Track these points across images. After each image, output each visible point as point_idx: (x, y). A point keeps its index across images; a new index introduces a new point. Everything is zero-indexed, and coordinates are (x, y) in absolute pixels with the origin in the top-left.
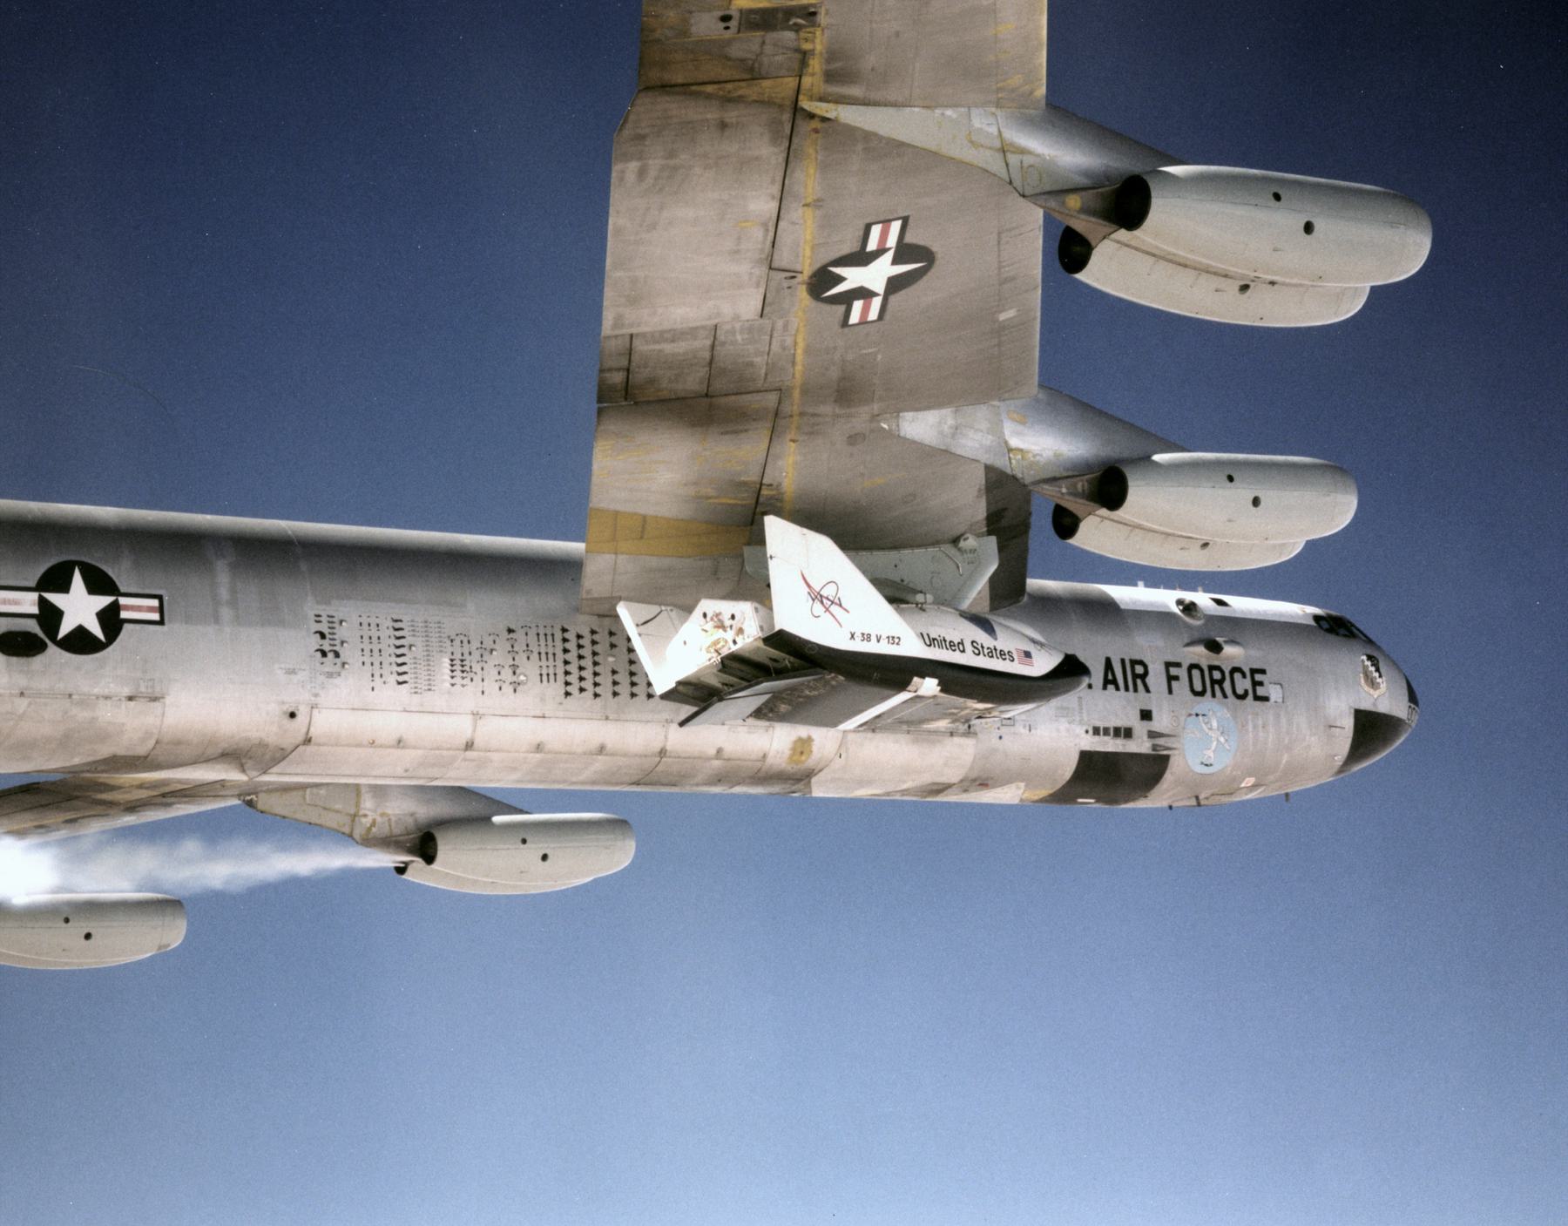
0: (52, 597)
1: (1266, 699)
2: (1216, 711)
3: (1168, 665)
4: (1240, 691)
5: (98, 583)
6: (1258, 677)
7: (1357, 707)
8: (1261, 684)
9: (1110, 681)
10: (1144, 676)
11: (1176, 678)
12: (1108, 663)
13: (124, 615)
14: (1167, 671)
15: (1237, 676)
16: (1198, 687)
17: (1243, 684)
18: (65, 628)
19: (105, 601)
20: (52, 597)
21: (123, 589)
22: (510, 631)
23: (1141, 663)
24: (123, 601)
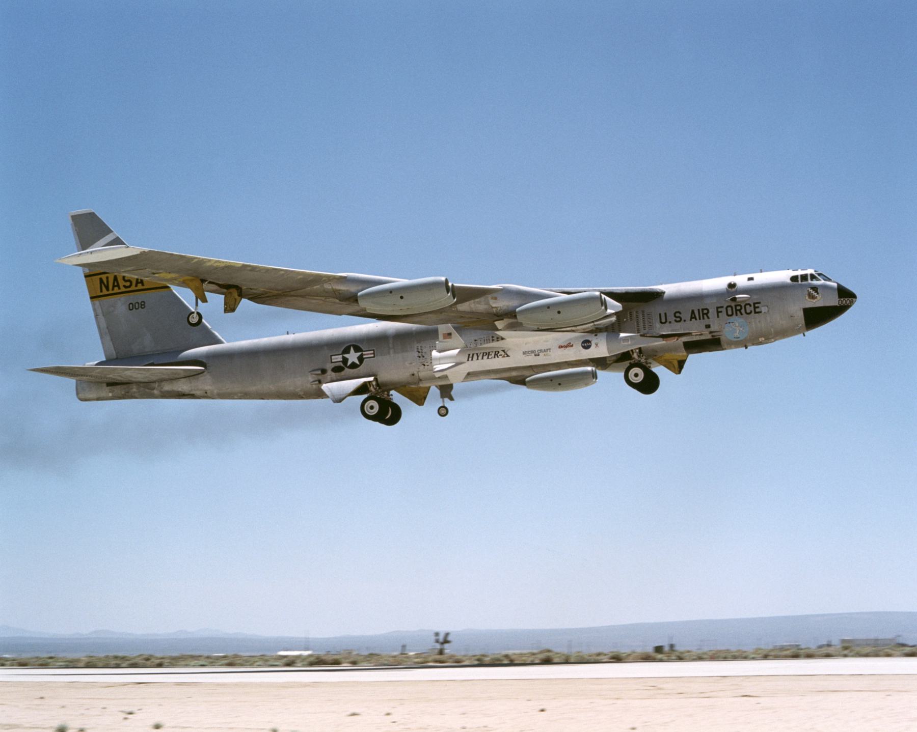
0: (345, 355)
1: (760, 312)
2: (737, 320)
3: (718, 308)
4: (748, 311)
5: (357, 349)
6: (756, 305)
7: (804, 307)
8: (758, 307)
9: (693, 317)
10: (707, 314)
11: (721, 312)
12: (693, 312)
13: (364, 357)
14: (717, 310)
15: (748, 307)
16: (730, 313)
17: (749, 309)
18: (349, 363)
19: (359, 354)
20: (345, 355)
21: (364, 350)
22: (475, 340)
23: (708, 310)
24: (364, 353)
